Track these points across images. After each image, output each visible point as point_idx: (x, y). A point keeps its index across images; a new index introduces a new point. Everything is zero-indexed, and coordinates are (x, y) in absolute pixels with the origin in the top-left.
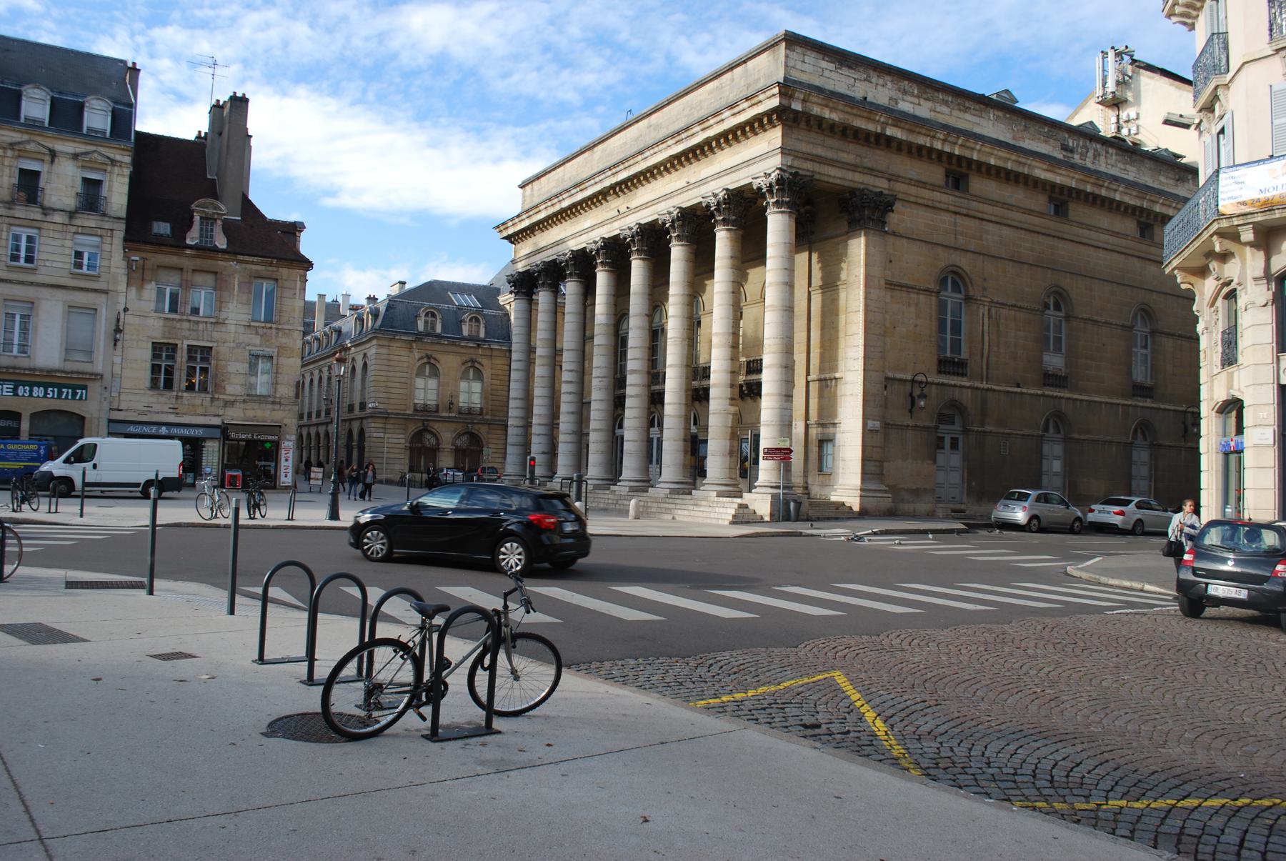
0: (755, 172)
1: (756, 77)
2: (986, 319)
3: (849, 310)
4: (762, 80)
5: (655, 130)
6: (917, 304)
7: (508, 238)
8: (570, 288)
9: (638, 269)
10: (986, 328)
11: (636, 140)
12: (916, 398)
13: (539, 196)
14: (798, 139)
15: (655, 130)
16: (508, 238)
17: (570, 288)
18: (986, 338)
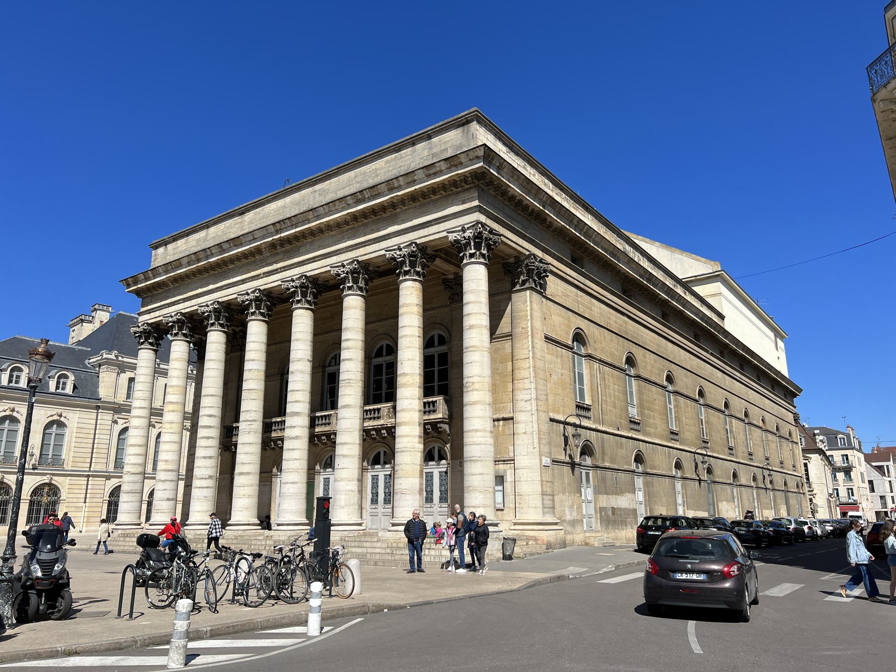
0: (413, 238)
1: (443, 147)
2: (598, 373)
3: (515, 358)
5: (320, 195)
6: (562, 356)
7: (138, 293)
8: (179, 349)
9: (216, 341)
10: (599, 383)
11: (298, 203)
12: (571, 436)
13: (174, 254)
14: (488, 202)
15: (320, 195)
16: (138, 293)
17: (179, 349)
18: (599, 389)
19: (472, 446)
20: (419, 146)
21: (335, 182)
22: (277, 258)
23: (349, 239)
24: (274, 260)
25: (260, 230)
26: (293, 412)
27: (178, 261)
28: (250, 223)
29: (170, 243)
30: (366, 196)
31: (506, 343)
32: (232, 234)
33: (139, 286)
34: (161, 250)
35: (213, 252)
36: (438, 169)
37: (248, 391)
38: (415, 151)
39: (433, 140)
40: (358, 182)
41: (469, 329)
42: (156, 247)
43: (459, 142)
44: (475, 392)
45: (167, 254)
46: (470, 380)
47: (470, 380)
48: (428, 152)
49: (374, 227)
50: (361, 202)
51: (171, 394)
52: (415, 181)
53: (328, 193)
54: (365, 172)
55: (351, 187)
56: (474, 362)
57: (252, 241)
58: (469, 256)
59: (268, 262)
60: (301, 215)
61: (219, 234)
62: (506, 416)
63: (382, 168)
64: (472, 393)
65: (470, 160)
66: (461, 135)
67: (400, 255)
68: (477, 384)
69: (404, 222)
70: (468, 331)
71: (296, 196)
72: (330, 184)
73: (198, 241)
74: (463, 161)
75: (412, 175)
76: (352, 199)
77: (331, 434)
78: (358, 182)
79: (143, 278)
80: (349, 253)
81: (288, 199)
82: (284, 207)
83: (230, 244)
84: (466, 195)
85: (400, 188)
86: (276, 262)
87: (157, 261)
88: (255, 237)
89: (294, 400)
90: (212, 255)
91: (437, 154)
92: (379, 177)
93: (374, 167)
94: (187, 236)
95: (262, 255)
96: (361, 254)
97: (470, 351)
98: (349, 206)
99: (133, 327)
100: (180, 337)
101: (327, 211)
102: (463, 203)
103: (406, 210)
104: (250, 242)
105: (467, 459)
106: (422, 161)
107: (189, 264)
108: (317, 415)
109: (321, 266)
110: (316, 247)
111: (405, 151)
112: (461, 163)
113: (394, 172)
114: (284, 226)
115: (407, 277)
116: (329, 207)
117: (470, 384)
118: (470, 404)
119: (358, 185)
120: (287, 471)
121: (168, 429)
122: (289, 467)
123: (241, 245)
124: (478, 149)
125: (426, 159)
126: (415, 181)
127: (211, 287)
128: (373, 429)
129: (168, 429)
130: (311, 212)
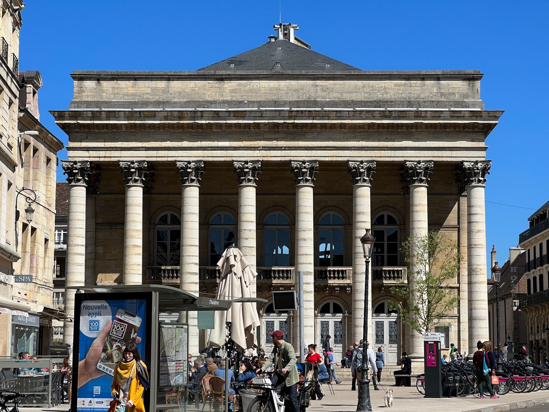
1: (451, 91)
4: (457, 96)
11: (296, 90)
19: (481, 310)
20: (428, 82)
21: (340, 84)
22: (277, 136)
23: (362, 140)
24: (273, 136)
25: (273, 112)
26: (308, 272)
27: (154, 113)
28: (233, 91)
29: (105, 79)
30: (393, 115)
31: (453, 232)
32: (207, 96)
33: (79, 121)
34: (90, 84)
35: (204, 115)
36: (462, 115)
37: (249, 248)
38: (424, 85)
39: (442, 82)
40: (366, 93)
41: (477, 232)
42: (81, 78)
43: (465, 92)
44: (482, 275)
45: (103, 91)
46: (479, 267)
47: (479, 267)
48: (437, 90)
49: (388, 137)
50: (386, 118)
51: (137, 238)
52: (440, 117)
53: (332, 91)
54: (373, 87)
55: (359, 94)
56: (481, 255)
57: (258, 118)
58: (478, 181)
59: (265, 137)
60: (324, 112)
61: (187, 90)
62: (452, 285)
63: (391, 89)
64: (480, 276)
65: (489, 116)
66: (467, 87)
67: (420, 167)
68: (483, 270)
69: (418, 140)
70: (477, 234)
71: (294, 83)
72: (335, 84)
73: (154, 90)
74: (483, 116)
75: (440, 113)
76: (379, 113)
77: (291, 286)
78: (366, 93)
79: (91, 115)
80: (364, 151)
81: (283, 83)
82: (278, 89)
83: (231, 113)
84: (474, 136)
85: (425, 118)
86: (277, 140)
87: (84, 94)
88: (263, 115)
89: (308, 262)
90: (202, 118)
91: (446, 95)
92: (388, 95)
93: (383, 85)
94: (135, 79)
95: (259, 129)
96: (376, 156)
97: (478, 248)
98: (374, 118)
99: (65, 162)
100: (139, 184)
101: (351, 115)
102: (472, 141)
103: (420, 131)
104: (255, 118)
105: (474, 318)
106: (431, 95)
107: (166, 118)
108: (273, 269)
109: (332, 155)
110: (325, 137)
111: (415, 82)
112: (481, 116)
113: (404, 95)
114: (300, 115)
115: (422, 184)
116: (354, 114)
117: (479, 270)
118: (479, 283)
119: (366, 95)
120: (306, 317)
121: (136, 270)
122: (308, 315)
123: (243, 118)
124: (498, 112)
125: (436, 95)
126: (440, 117)
127: (186, 144)
128: (337, 286)
129: (136, 270)
130: (335, 112)
